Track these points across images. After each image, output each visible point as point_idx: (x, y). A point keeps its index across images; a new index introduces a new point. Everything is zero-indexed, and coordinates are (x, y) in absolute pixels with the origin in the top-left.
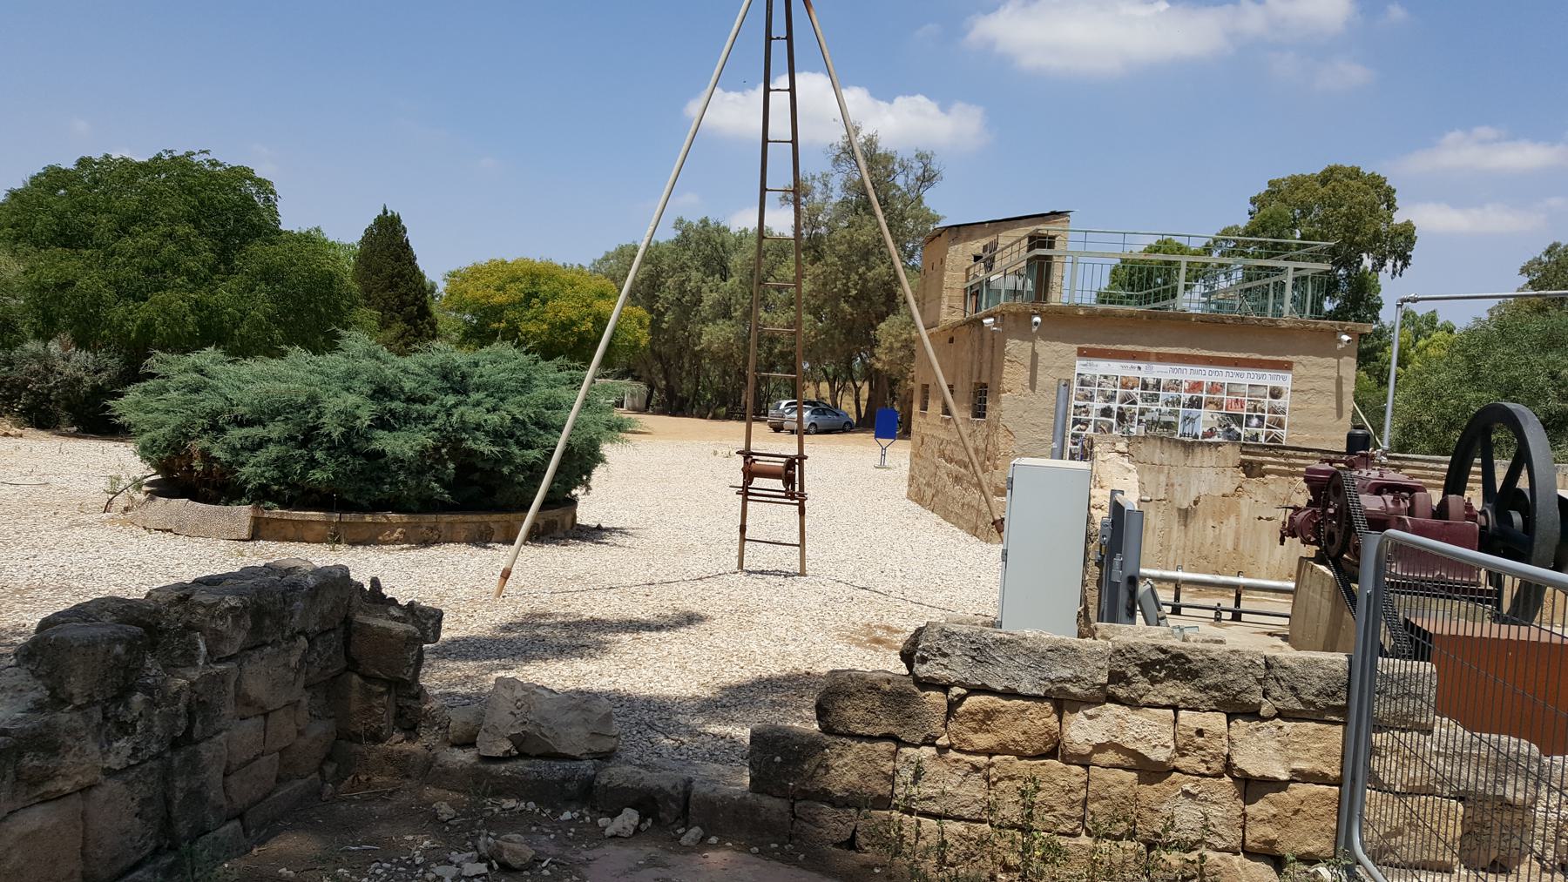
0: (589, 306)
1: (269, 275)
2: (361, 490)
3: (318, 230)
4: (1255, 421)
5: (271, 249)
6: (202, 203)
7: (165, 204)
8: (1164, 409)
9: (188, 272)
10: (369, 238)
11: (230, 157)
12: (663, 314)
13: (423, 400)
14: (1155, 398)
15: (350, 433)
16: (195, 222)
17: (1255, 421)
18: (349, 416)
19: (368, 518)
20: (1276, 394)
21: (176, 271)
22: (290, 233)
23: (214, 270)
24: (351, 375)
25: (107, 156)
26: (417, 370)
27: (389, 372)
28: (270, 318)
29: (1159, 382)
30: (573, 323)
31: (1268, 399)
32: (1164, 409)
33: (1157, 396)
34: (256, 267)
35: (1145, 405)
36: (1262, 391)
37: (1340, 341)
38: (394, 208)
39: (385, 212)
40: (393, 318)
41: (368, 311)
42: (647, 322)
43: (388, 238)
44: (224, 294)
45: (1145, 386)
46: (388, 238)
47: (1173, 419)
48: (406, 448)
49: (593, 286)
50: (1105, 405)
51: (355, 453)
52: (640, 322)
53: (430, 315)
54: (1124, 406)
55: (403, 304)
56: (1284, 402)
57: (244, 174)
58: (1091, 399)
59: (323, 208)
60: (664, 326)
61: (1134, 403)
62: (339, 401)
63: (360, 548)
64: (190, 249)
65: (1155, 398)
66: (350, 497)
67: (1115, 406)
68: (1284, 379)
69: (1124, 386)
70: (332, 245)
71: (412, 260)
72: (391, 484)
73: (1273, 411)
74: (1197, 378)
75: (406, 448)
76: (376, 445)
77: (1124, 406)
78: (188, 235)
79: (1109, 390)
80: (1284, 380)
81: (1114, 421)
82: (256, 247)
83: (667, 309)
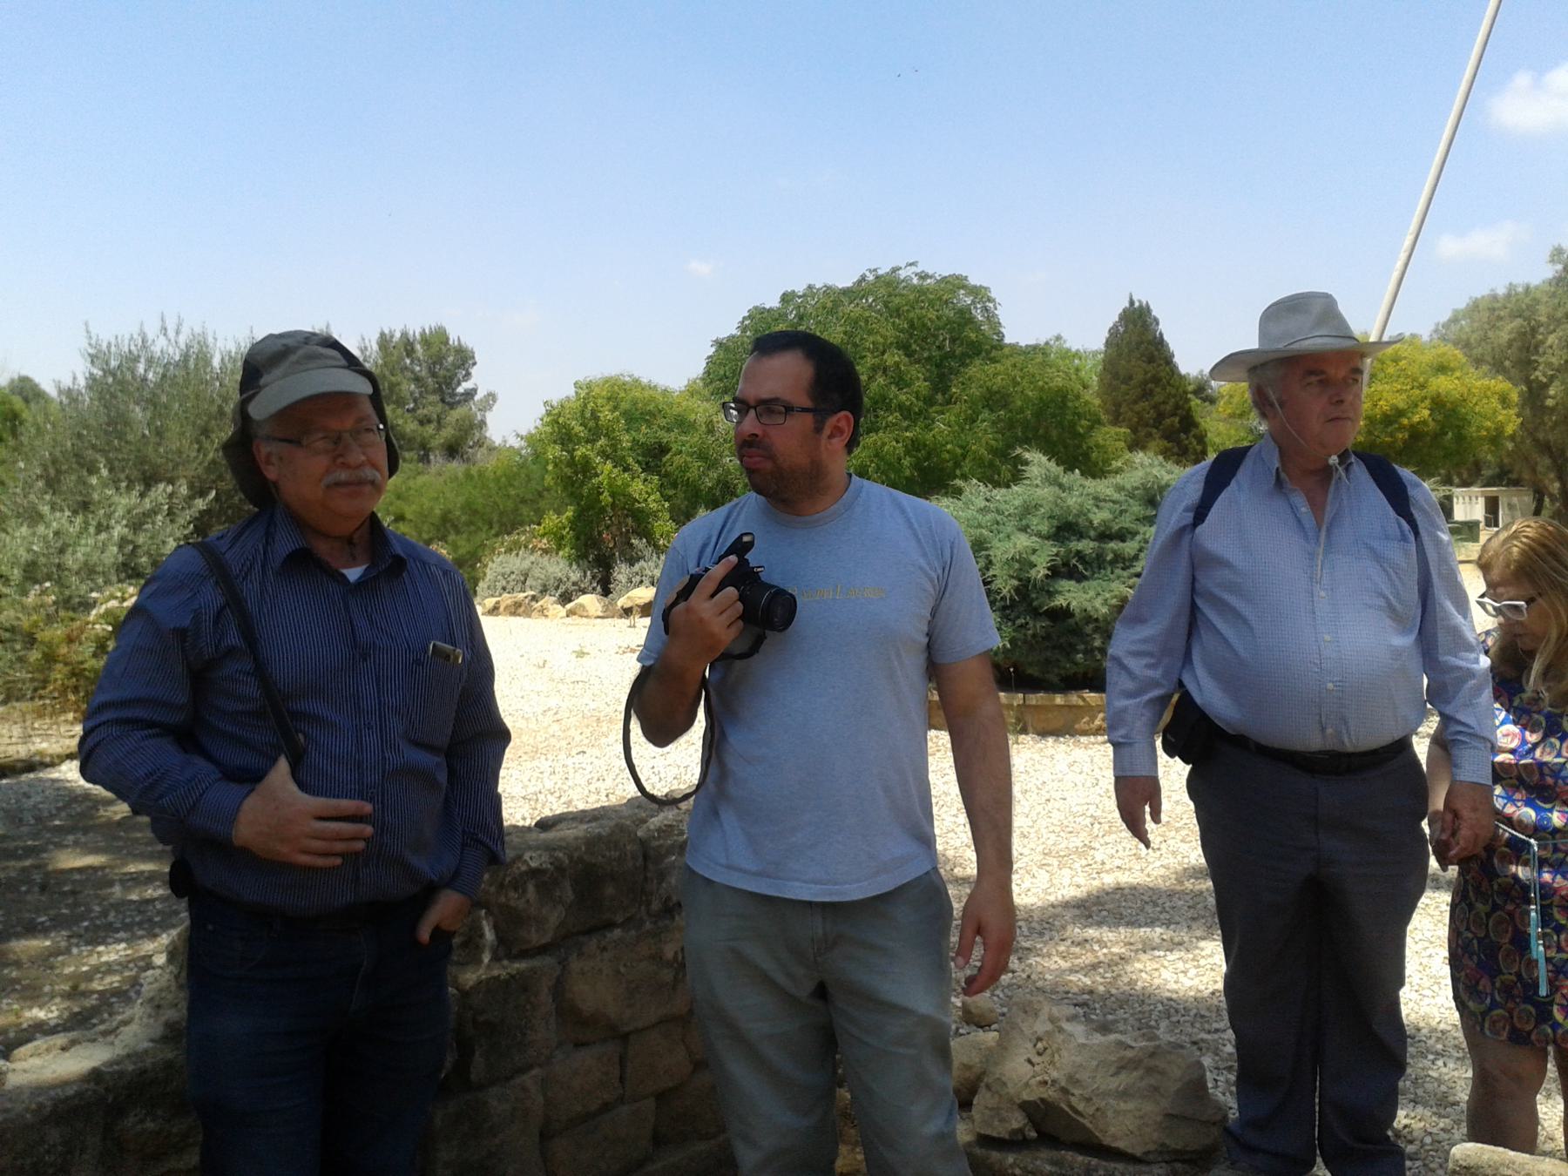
0: (1422, 386)
1: (994, 399)
2: (1048, 661)
3: (1058, 338)
5: (990, 368)
6: (912, 326)
7: (870, 333)
9: (900, 407)
10: (1115, 340)
11: (939, 265)
12: (1546, 386)
13: (1122, 536)
15: (1025, 589)
16: (905, 347)
18: (1023, 563)
19: (1059, 699)
21: (888, 409)
22: (1013, 347)
23: (930, 401)
24: (1028, 509)
25: (810, 287)
26: (1116, 496)
27: (1072, 501)
28: (994, 451)
30: (1400, 413)
34: (975, 391)
38: (1141, 297)
39: (1132, 303)
40: (1150, 435)
41: (1113, 430)
42: (1514, 397)
43: (1138, 337)
44: (942, 427)
46: (1138, 337)
48: (1098, 603)
49: (1428, 357)
51: (1036, 613)
52: (1504, 400)
53: (1196, 425)
55: (1161, 416)
57: (956, 283)
59: (1053, 310)
60: (1550, 402)
62: (1008, 545)
63: (1051, 739)
64: (901, 382)
66: (1033, 671)
70: (1077, 355)
71: (1168, 360)
72: (1085, 652)
75: (1098, 603)
76: (1060, 601)
78: (897, 364)
82: (975, 369)
83: (1552, 379)
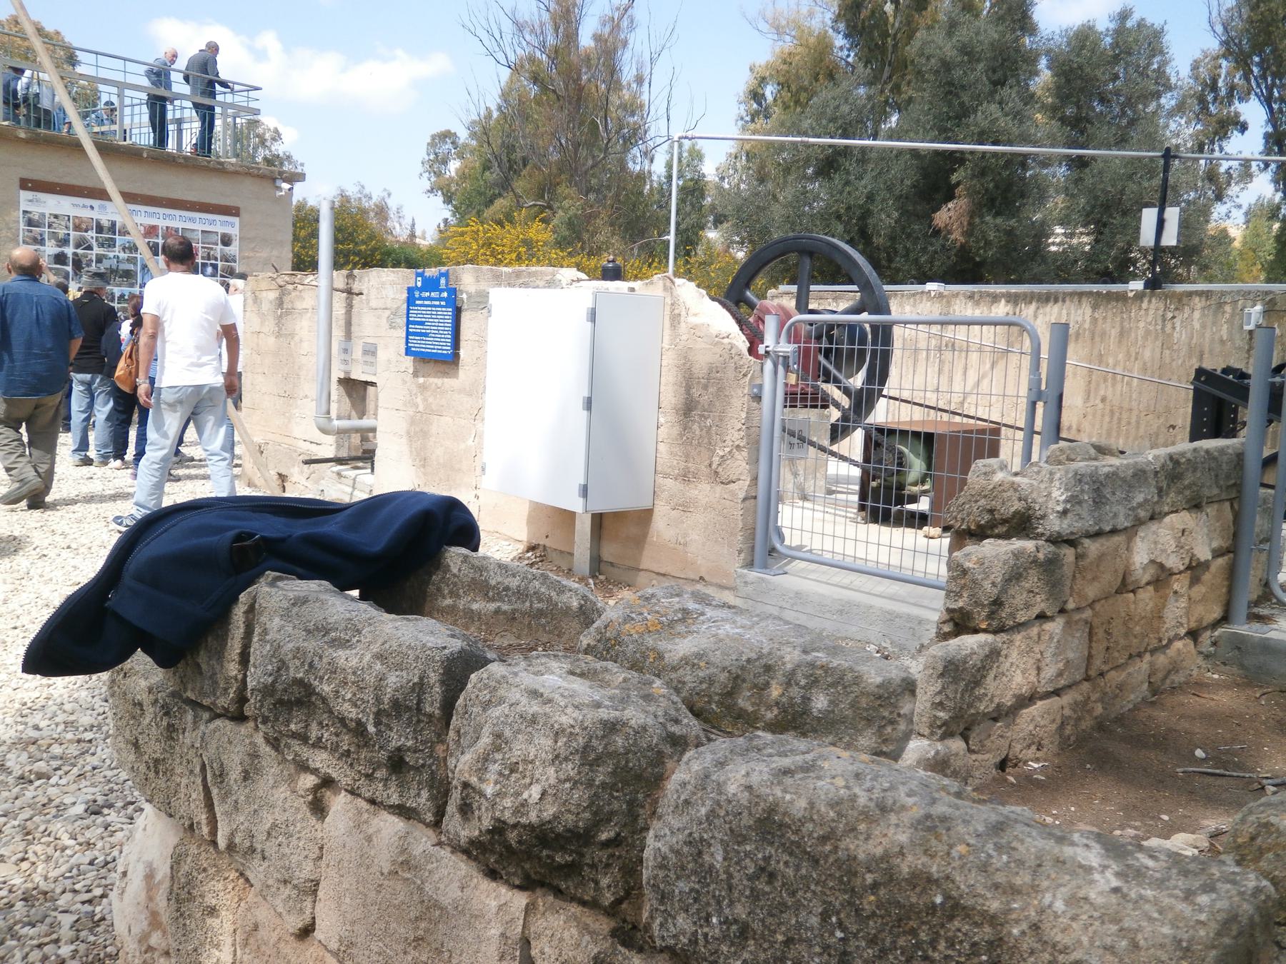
4: (209, 270)
8: (122, 255)
14: (111, 243)
17: (209, 270)
20: (226, 241)
29: (114, 224)
31: (220, 246)
32: (122, 255)
33: (114, 240)
35: (101, 251)
36: (213, 238)
37: (280, 189)
45: (100, 229)
47: (131, 267)
50: (57, 250)
54: (80, 251)
56: (233, 249)
58: (42, 242)
61: (90, 248)
65: (111, 243)
67: (69, 251)
68: (233, 225)
69: (77, 228)
73: (225, 259)
74: (153, 222)
77: (80, 251)
79: (62, 232)
80: (231, 226)
81: (69, 268)
